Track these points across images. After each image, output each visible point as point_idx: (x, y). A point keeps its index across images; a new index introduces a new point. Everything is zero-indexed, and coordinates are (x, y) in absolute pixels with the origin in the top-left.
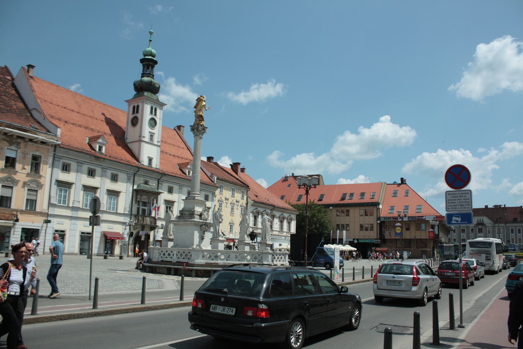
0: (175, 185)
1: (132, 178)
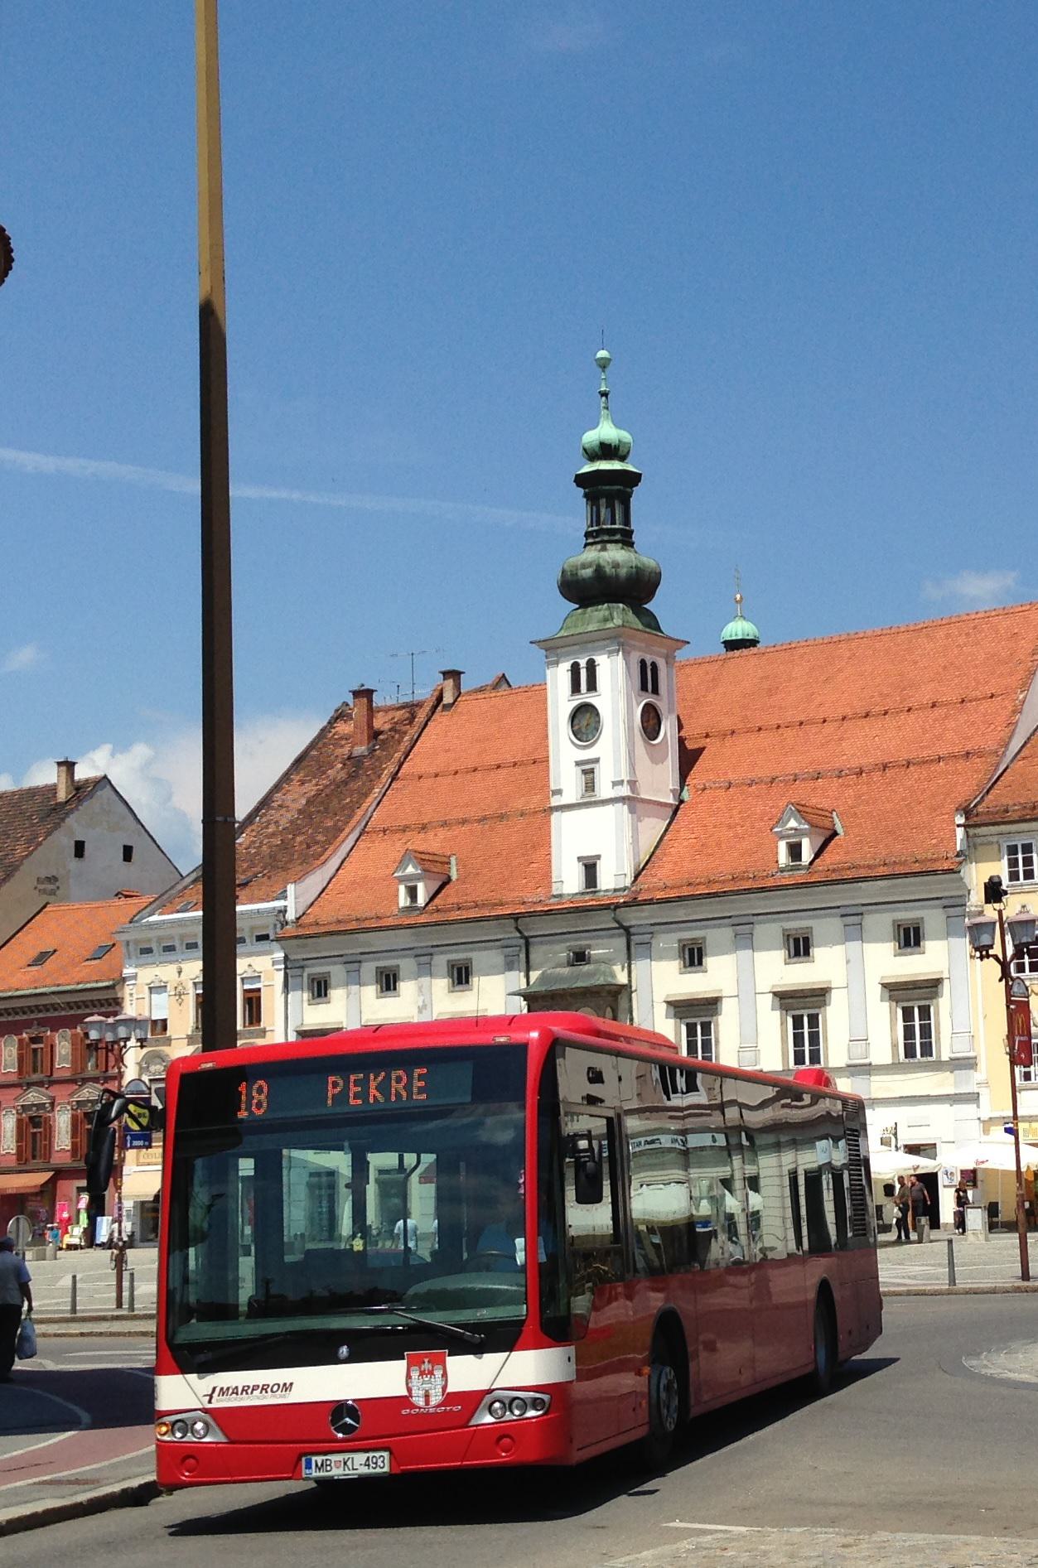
0: (706, 927)
1: (523, 956)
